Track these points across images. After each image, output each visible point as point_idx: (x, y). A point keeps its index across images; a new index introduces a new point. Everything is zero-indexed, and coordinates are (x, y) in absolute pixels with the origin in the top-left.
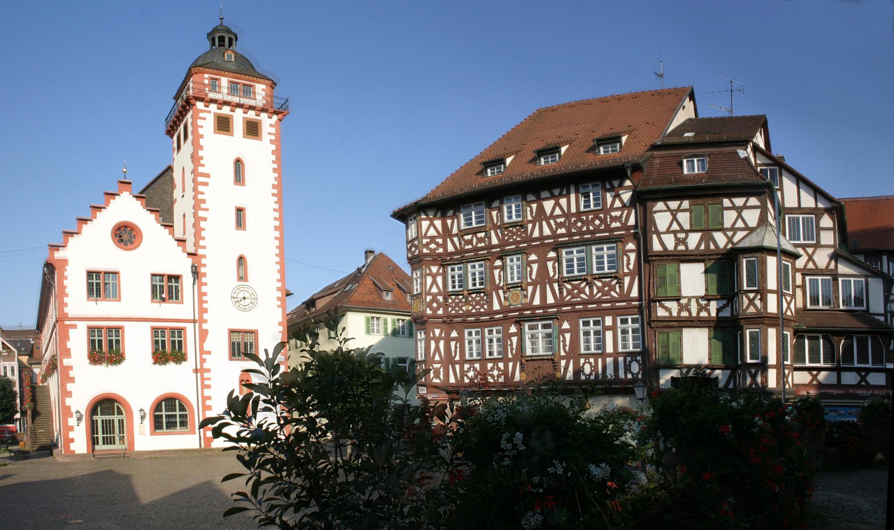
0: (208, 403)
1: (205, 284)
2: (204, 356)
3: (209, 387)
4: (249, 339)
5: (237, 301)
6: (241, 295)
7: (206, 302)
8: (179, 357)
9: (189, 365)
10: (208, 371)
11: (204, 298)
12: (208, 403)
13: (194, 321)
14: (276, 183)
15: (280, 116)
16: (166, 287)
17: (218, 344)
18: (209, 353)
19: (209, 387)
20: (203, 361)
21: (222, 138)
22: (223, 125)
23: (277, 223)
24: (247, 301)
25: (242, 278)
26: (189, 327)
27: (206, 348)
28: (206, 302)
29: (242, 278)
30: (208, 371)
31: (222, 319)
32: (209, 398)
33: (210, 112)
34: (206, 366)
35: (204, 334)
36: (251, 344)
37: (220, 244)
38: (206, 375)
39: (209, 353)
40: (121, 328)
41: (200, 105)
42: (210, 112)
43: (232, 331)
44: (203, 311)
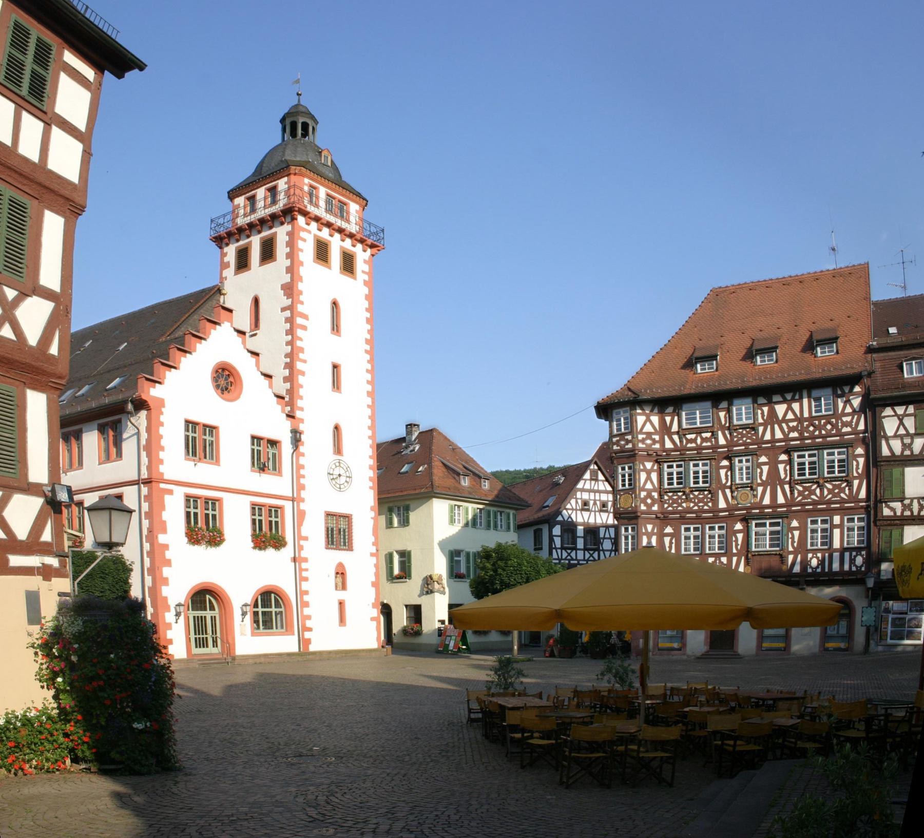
0: (306, 598)
1: (303, 455)
2: (302, 542)
3: (306, 579)
4: (343, 524)
5: (333, 478)
6: (337, 472)
7: (303, 477)
8: (278, 543)
9: (287, 552)
10: (306, 560)
11: (302, 472)
12: (306, 598)
13: (293, 500)
14: (368, 337)
15: (375, 250)
16: (264, 455)
17: (315, 529)
18: (306, 539)
19: (306, 579)
20: (301, 548)
21: (320, 268)
22: (322, 252)
23: (369, 388)
24: (342, 480)
25: (338, 450)
26: (288, 505)
27: (303, 534)
28: (303, 477)
29: (338, 450)
30: (306, 560)
31: (319, 501)
32: (306, 593)
33: (309, 232)
34: (303, 554)
35: (300, 516)
36: (344, 531)
37: (318, 406)
38: (304, 565)
39: (306, 539)
40: (219, 500)
41: (301, 220)
42: (309, 232)
43: (329, 515)
44: (302, 487)
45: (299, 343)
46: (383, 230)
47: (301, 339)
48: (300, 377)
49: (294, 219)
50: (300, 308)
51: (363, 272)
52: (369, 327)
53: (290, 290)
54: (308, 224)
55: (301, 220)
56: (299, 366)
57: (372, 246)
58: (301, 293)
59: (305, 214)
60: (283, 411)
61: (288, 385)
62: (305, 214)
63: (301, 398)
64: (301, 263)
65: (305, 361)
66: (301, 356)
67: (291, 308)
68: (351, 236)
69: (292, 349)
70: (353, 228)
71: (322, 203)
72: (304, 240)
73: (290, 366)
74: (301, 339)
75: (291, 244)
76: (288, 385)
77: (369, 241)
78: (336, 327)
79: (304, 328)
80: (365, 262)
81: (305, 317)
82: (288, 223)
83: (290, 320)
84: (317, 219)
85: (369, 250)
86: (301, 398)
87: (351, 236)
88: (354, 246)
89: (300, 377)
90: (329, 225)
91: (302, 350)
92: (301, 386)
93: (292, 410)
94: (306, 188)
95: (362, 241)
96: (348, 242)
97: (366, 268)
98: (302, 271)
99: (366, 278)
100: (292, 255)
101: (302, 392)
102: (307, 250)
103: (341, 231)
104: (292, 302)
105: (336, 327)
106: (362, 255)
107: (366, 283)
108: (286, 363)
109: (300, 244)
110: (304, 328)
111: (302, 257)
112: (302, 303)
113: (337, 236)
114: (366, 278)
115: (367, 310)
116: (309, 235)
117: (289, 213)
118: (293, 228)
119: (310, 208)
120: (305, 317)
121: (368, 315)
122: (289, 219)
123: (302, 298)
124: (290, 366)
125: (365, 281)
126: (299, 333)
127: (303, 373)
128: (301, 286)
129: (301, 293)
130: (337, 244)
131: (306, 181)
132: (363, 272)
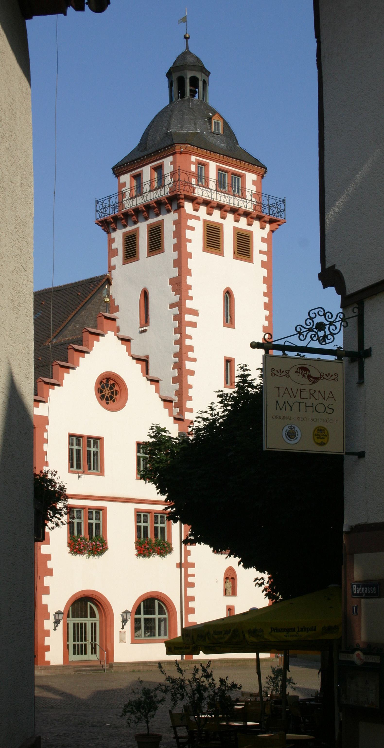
15: (275, 225)
33: (198, 218)
41: (188, 207)
42: (198, 218)
45: (188, 342)
46: (284, 201)
47: (190, 337)
48: (189, 377)
49: (180, 207)
50: (189, 304)
51: (261, 252)
52: (267, 313)
53: (179, 285)
54: (196, 210)
55: (188, 207)
56: (189, 365)
57: (271, 222)
58: (190, 287)
59: (193, 200)
60: (170, 415)
61: (177, 386)
62: (193, 200)
63: (190, 399)
64: (190, 255)
65: (194, 360)
66: (191, 355)
67: (179, 305)
68: (246, 214)
69: (181, 348)
70: (249, 208)
71: (212, 185)
72: (192, 229)
73: (179, 366)
74: (190, 337)
75: (179, 234)
76: (177, 386)
77: (267, 218)
78: (229, 319)
79: (194, 325)
80: (263, 240)
81: (195, 313)
82: (175, 211)
83: (179, 318)
84: (206, 203)
85: (268, 226)
86: (190, 399)
87: (246, 214)
88: (250, 224)
89: (189, 377)
90: (220, 207)
91: (191, 348)
92: (191, 387)
93: (181, 413)
94: (193, 168)
95: (259, 218)
96: (243, 220)
97: (264, 247)
98: (191, 264)
99: (265, 258)
100: (180, 247)
101: (191, 392)
102: (195, 237)
103: (234, 211)
104: (181, 299)
105: (229, 319)
106: (259, 233)
107: (264, 265)
108: (175, 363)
109: (188, 234)
110: (194, 325)
111: (190, 247)
112: (191, 298)
113: (230, 217)
114: (265, 258)
115: (265, 294)
116: (197, 220)
117: (173, 202)
118: (180, 216)
119: (200, 193)
120: (195, 313)
121: (266, 300)
122: (175, 206)
123: (190, 293)
124: (179, 366)
125: (263, 262)
126: (189, 330)
127: (192, 373)
128: (189, 280)
129: (190, 287)
130: (229, 226)
131: (194, 158)
132: (261, 252)
